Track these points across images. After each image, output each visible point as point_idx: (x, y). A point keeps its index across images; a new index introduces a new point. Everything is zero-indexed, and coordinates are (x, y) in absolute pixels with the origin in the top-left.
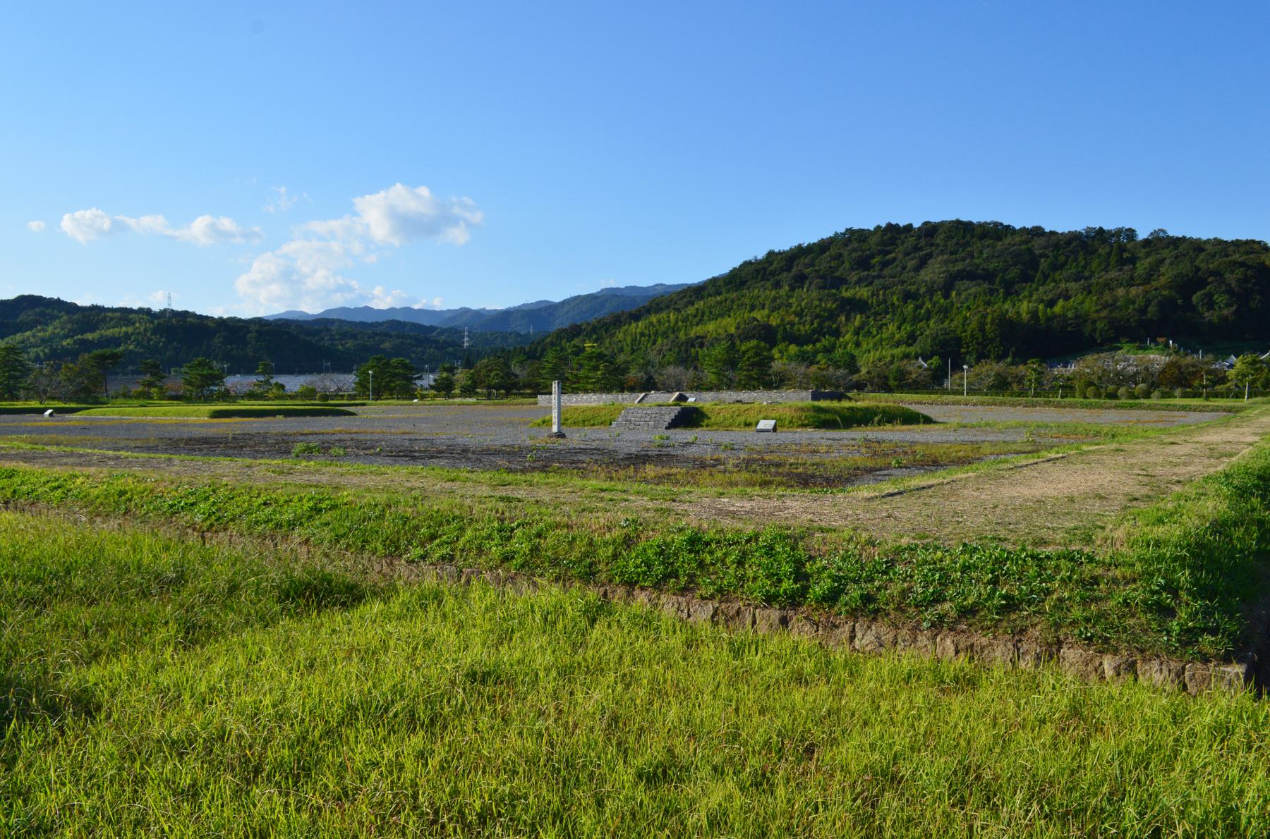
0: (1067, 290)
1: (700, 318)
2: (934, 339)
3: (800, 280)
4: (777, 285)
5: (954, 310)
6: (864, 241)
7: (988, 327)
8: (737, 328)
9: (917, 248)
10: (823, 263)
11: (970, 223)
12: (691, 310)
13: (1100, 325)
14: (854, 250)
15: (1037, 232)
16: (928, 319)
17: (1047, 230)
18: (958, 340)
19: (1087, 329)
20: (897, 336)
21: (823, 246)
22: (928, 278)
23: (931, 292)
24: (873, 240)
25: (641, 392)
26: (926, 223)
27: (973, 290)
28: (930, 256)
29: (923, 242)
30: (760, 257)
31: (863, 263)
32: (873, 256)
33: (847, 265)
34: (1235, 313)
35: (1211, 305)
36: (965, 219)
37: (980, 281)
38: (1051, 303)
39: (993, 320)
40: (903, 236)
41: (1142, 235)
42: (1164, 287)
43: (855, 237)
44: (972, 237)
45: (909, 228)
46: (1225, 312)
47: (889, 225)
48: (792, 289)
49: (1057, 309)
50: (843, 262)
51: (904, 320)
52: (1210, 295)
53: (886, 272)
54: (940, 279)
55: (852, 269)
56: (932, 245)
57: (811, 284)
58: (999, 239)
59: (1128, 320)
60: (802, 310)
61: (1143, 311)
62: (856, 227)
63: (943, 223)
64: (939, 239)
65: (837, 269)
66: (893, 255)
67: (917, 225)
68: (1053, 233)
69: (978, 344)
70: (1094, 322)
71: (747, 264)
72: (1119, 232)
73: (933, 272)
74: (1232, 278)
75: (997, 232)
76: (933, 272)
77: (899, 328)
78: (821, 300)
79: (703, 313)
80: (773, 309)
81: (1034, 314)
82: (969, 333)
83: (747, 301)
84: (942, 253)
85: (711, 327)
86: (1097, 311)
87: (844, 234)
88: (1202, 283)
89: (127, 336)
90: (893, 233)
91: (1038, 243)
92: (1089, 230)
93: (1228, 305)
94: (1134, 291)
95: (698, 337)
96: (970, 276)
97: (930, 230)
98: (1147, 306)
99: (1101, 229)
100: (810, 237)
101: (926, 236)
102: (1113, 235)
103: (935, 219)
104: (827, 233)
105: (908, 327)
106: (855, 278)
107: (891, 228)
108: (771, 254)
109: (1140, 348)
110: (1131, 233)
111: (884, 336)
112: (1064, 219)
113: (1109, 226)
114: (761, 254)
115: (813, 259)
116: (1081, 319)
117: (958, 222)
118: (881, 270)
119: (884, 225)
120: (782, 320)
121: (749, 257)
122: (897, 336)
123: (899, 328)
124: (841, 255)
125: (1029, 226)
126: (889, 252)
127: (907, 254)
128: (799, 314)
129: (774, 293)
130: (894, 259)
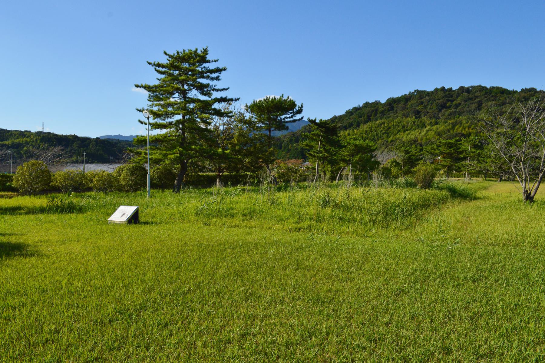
17: (538, 90)
21: (406, 99)
30: (361, 105)
31: (444, 106)
33: (435, 107)
36: (483, 85)
45: (451, 89)
62: (419, 90)
87: (414, 93)
89: (27, 143)
100: (397, 94)
108: (367, 104)
124: (422, 103)
125: (528, 87)
126: (452, 101)
130: (460, 104)
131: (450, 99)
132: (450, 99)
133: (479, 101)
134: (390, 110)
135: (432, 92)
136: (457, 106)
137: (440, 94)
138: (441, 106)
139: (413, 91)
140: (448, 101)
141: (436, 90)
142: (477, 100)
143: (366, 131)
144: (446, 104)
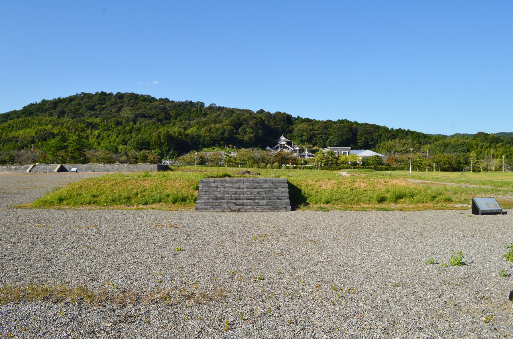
0: (190, 124)
1: (11, 128)
2: (137, 142)
3: (62, 113)
4: (51, 115)
5: (143, 130)
6: (90, 98)
7: (162, 137)
8: (36, 133)
9: (116, 103)
10: (72, 106)
11: (138, 95)
12: (6, 124)
13: (207, 139)
14: (86, 102)
15: (166, 100)
16: (131, 133)
17: (170, 100)
18: (149, 143)
19: (202, 140)
20: (117, 140)
21: (71, 99)
22: (126, 116)
23: (128, 122)
24: (95, 99)
25: (30, 164)
26: (118, 93)
27: (147, 122)
28: (122, 107)
29: (118, 101)
32: (96, 105)
33: (84, 109)
34: (255, 136)
35: (245, 133)
36: (135, 93)
37: (149, 119)
38: (185, 129)
39: (164, 134)
40: (109, 97)
41: (207, 105)
42: (228, 125)
43: (86, 96)
44: (140, 100)
45: (111, 94)
46: (251, 135)
47: (102, 92)
48: (59, 117)
49: (189, 132)
50: (82, 107)
51: (120, 133)
52: (245, 129)
53: (102, 112)
54: (132, 116)
55: (87, 110)
56: (123, 102)
57: (68, 115)
58: (151, 102)
59: (218, 137)
60: (69, 127)
61: (223, 134)
62: (86, 92)
63: (126, 94)
64: (126, 100)
65: (80, 109)
66: (105, 105)
67: (114, 93)
68: (172, 101)
69: (158, 145)
70: (204, 137)
71: (31, 105)
72: (198, 103)
73: (126, 113)
74: (252, 122)
75: (149, 99)
76: (126, 113)
77: (117, 137)
78: (78, 122)
79: (13, 127)
80: (54, 125)
81: (180, 134)
82: (153, 140)
83: (36, 121)
84: (127, 106)
85: (21, 132)
86: (205, 133)
87: (81, 95)
88: (241, 125)
90: (103, 96)
91: (167, 105)
92: (187, 101)
93: (252, 133)
94: (218, 125)
95: (14, 137)
96: (144, 116)
97: (120, 96)
98: (224, 132)
99: (191, 101)
100: (65, 94)
101: (119, 98)
102: (195, 104)
103: (123, 91)
104: (73, 94)
105: (121, 137)
106: (89, 114)
107: (103, 93)
108: (44, 101)
109: (223, 149)
110: (202, 104)
111: (112, 140)
112: (178, 96)
113: (195, 100)
114: (39, 101)
115: (67, 105)
116: (199, 136)
117: (133, 94)
118: (101, 111)
119: (100, 92)
120: (60, 131)
121: (33, 102)
122: (117, 140)
123: (117, 137)
124: (80, 104)
125: (163, 98)
126: (103, 104)
127: (112, 105)
128: (68, 128)
129: (50, 118)
130: (106, 107)
131: (103, 102)
132: (103, 102)
133: (121, 106)
134: (53, 109)
135: (94, 95)
136: (103, 109)
137: (97, 97)
138: (89, 108)
139: (80, 93)
140: (100, 104)
141: (97, 93)
142: (119, 105)
143: (5, 127)
144: (93, 106)
